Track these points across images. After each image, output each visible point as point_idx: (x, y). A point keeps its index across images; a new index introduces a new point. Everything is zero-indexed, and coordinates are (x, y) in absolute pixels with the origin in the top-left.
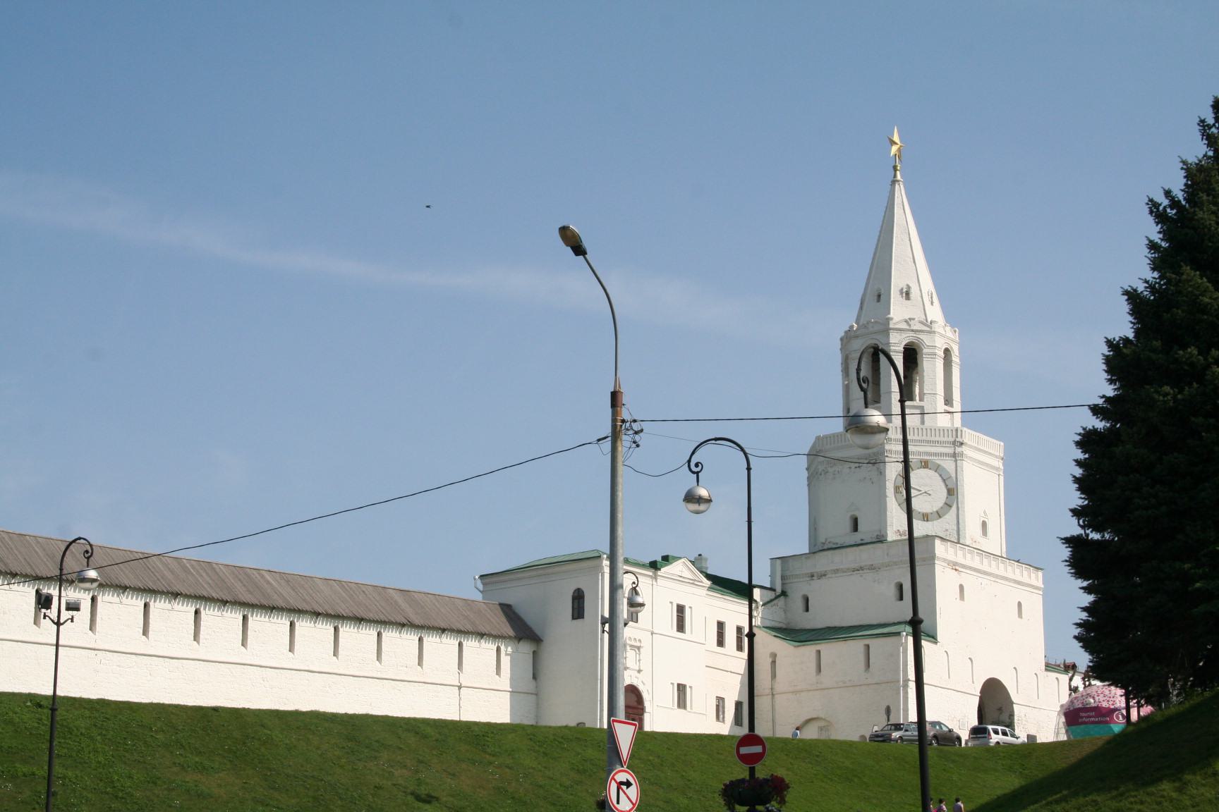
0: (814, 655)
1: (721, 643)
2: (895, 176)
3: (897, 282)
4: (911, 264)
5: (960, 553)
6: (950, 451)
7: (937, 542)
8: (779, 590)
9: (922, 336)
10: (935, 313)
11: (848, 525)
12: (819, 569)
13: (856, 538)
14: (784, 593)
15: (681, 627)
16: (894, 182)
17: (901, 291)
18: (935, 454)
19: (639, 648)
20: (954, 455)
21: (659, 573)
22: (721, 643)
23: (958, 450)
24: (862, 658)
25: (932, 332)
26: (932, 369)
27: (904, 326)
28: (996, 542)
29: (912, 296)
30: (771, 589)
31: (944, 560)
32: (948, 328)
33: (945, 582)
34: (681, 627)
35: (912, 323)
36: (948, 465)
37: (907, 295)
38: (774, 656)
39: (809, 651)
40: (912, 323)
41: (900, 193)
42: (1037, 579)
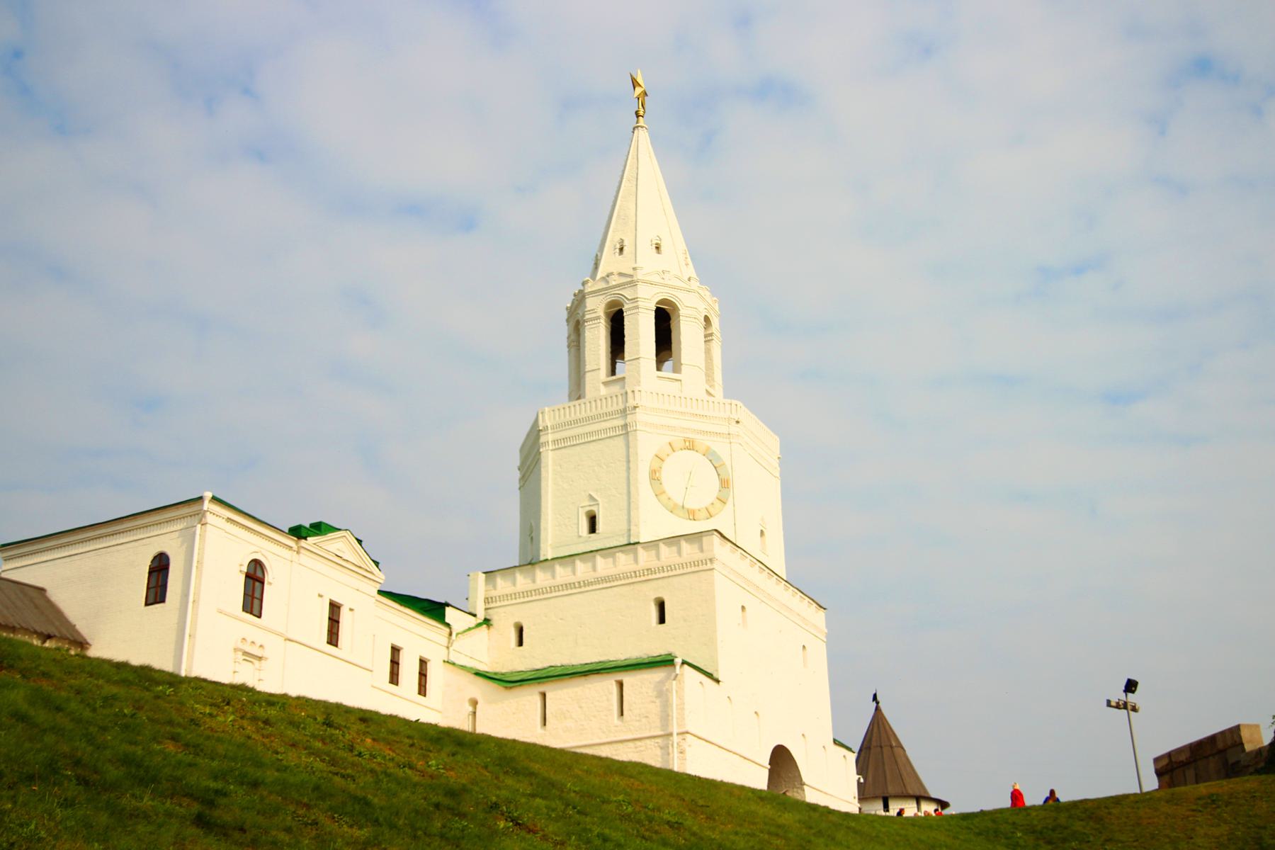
1: (394, 678)
9: (680, 294)
11: (584, 524)
13: (595, 542)
14: (487, 621)
15: (333, 638)
19: (260, 658)
21: (303, 543)
22: (394, 678)
27: (657, 279)
34: (333, 638)
36: (720, 447)
38: (474, 703)
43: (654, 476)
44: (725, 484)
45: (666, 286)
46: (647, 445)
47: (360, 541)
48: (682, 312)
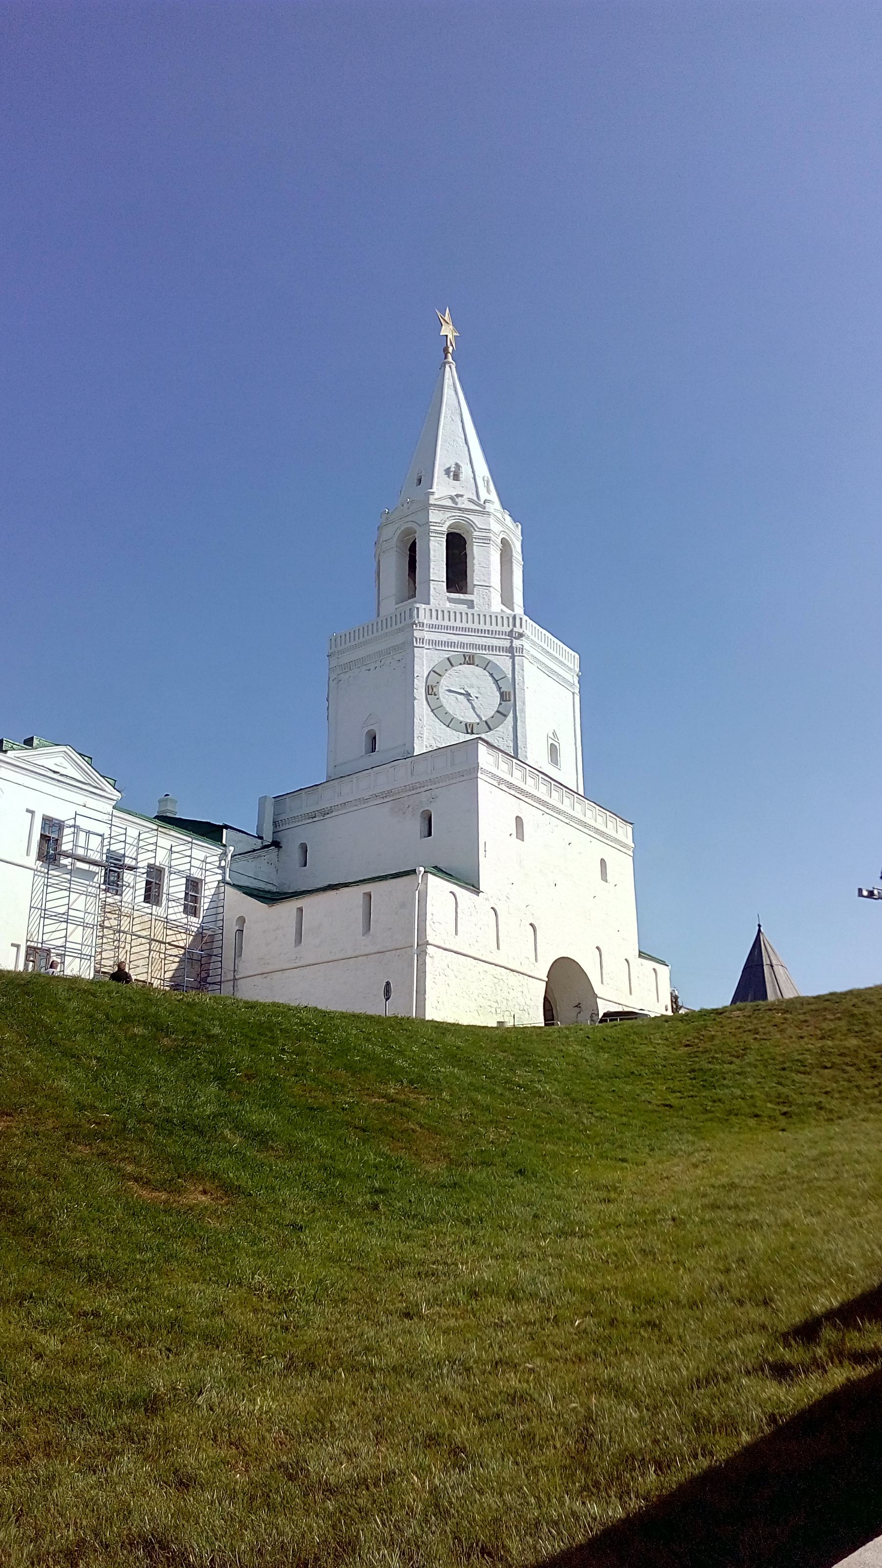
0: (295, 912)
2: (446, 357)
3: (443, 459)
4: (458, 436)
5: (517, 774)
6: (507, 644)
7: (482, 748)
8: (268, 839)
10: (490, 495)
11: (362, 743)
12: (325, 805)
16: (444, 365)
17: (447, 471)
18: (484, 647)
20: (511, 650)
23: (517, 643)
24: (359, 913)
25: (484, 513)
26: (485, 564)
27: (449, 503)
28: (570, 771)
29: (462, 476)
30: (261, 838)
31: (494, 776)
32: (508, 519)
33: (494, 809)
35: (458, 500)
36: (503, 662)
37: (456, 477)
38: (242, 920)
39: (288, 908)
40: (458, 500)
41: (451, 375)
42: (625, 834)
43: (430, 690)
44: (504, 697)
45: (459, 509)
46: (424, 662)
47: (90, 760)
48: (475, 533)
